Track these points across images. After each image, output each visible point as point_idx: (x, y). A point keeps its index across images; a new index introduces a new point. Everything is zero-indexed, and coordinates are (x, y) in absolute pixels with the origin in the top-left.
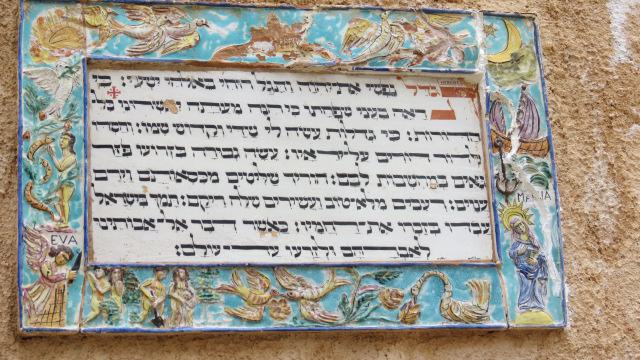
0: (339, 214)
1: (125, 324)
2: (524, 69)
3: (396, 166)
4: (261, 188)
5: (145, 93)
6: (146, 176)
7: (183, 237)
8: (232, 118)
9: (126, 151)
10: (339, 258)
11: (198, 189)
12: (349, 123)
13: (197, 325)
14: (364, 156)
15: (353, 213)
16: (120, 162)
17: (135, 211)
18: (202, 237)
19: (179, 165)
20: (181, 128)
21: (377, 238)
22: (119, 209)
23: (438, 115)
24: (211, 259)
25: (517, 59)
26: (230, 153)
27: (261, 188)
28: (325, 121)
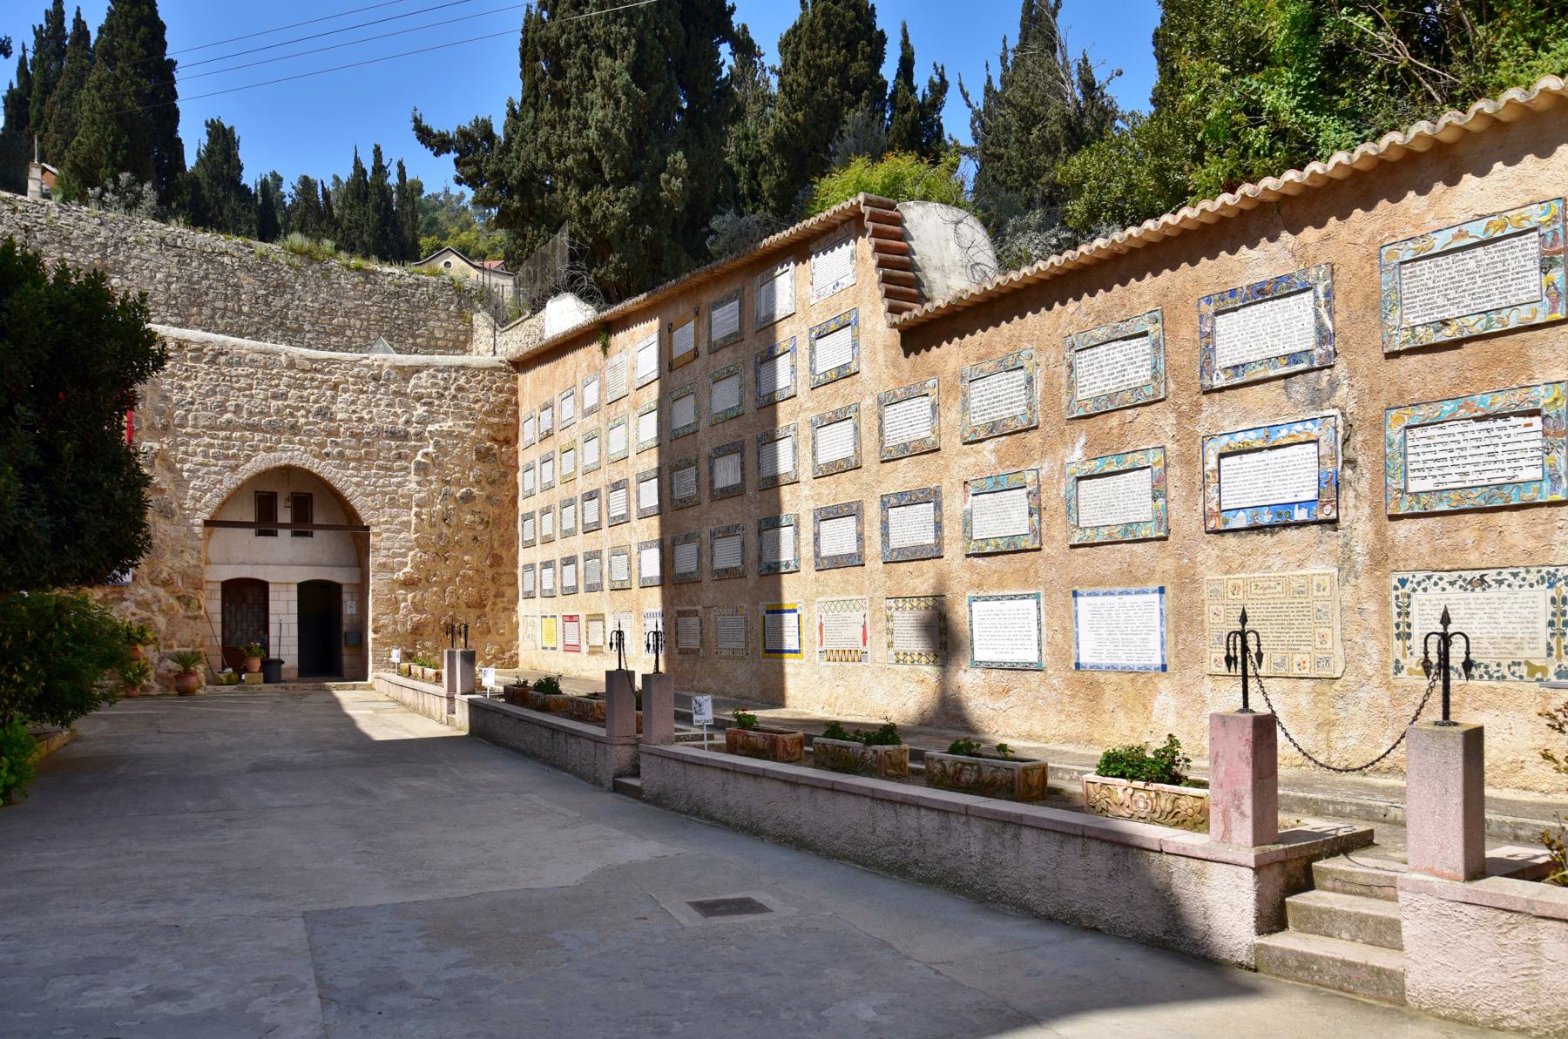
0: (1487, 467)
1: (1416, 510)
2: (1559, 403)
3: (1509, 447)
4: (1462, 461)
5: (1424, 434)
6: (1425, 462)
7: (1436, 481)
8: (1452, 439)
9: (1418, 454)
10: (1486, 483)
11: (1440, 464)
12: (1493, 434)
13: (1437, 509)
14: (1497, 445)
15: (1493, 466)
16: (1417, 458)
17: (1422, 474)
18: (1442, 480)
19: (1435, 457)
20: (1435, 444)
21: (1500, 474)
22: (1416, 474)
23: (1526, 425)
24: (1444, 487)
25: (1556, 399)
26: (1451, 451)
27: (1462, 461)
28: (1485, 434)
